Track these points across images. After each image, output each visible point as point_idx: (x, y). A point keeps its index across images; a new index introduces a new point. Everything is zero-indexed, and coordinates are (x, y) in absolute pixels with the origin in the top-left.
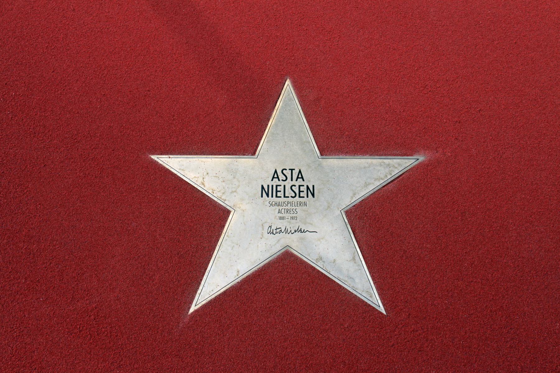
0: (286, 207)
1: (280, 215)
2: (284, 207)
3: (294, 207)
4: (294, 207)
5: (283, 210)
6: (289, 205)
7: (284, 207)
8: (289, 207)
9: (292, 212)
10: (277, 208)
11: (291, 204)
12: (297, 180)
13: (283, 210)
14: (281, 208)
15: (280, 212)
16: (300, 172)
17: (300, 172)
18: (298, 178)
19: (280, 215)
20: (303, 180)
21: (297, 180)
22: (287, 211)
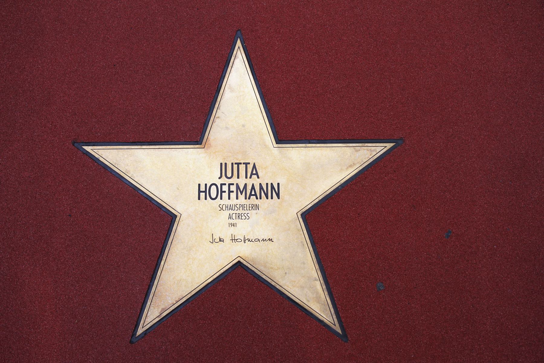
1: (231, 221)
2: (235, 212)
4: (246, 212)
5: (234, 215)
7: (235, 212)
10: (227, 213)
11: (243, 206)
12: (250, 178)
14: (231, 212)
15: (230, 217)
16: (254, 166)
17: (254, 166)
19: (231, 221)
20: (258, 177)
21: (250, 178)
22: (239, 216)
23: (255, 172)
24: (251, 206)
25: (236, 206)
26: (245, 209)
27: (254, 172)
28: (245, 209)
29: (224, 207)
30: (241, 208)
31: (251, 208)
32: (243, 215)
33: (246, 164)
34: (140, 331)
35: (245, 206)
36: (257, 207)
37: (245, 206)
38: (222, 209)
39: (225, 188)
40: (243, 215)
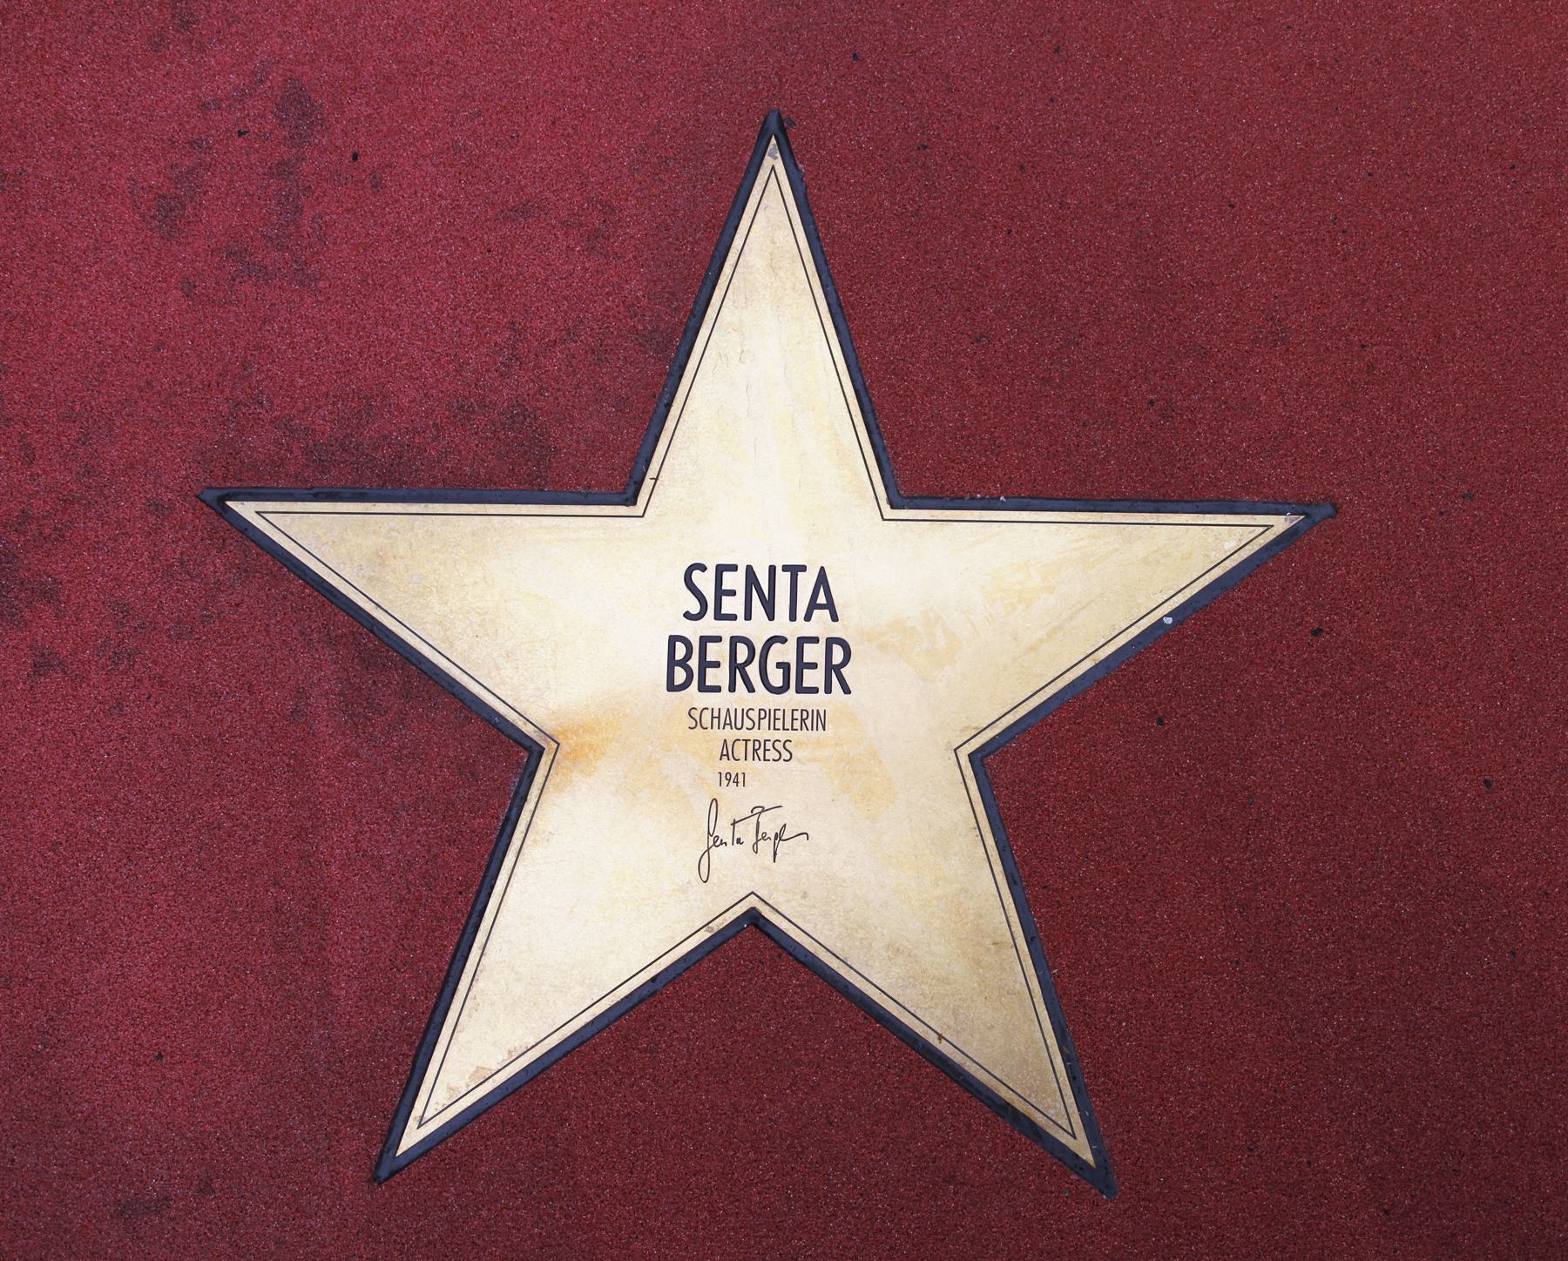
0: (752, 735)
1: (727, 766)
2: (744, 734)
3: (782, 735)
4: (782, 735)
5: (740, 746)
6: (765, 723)
8: (763, 733)
9: (772, 754)
12: (808, 618)
13: (740, 746)
14: (730, 734)
15: (726, 753)
16: (822, 579)
17: (822, 579)
18: (813, 605)
20: (835, 618)
21: (808, 618)
22: (758, 750)
23: (824, 598)
24: (797, 715)
25: (746, 713)
26: (779, 724)
27: (822, 599)
28: (779, 724)
29: (707, 716)
30: (765, 723)
31: (797, 724)
32: (769, 746)
33: (795, 570)
34: (412, 1137)
35: (779, 714)
36: (819, 720)
37: (779, 714)
38: (699, 723)
39: (717, 652)
40: (769, 746)
